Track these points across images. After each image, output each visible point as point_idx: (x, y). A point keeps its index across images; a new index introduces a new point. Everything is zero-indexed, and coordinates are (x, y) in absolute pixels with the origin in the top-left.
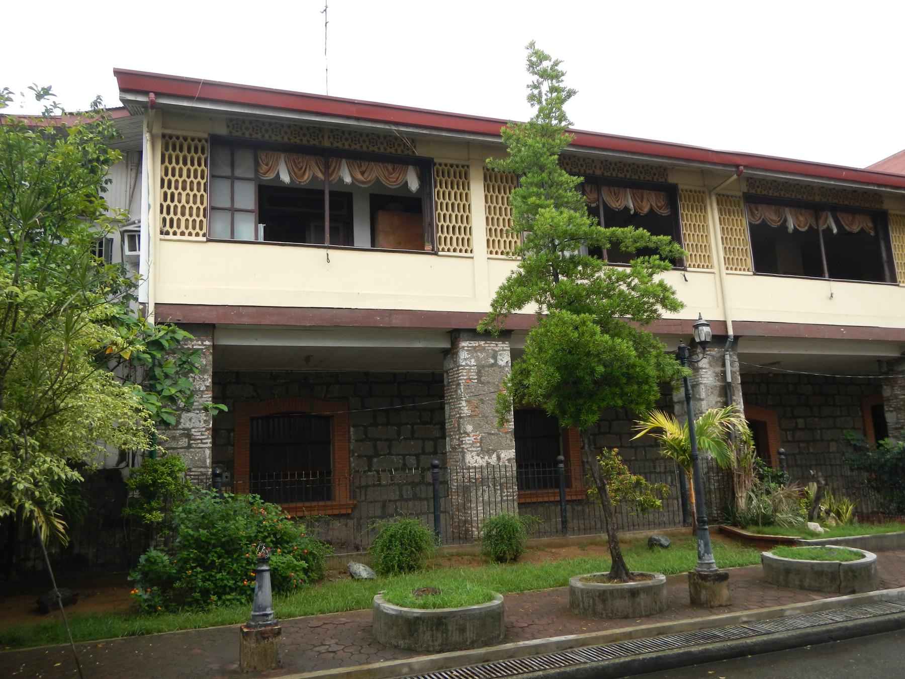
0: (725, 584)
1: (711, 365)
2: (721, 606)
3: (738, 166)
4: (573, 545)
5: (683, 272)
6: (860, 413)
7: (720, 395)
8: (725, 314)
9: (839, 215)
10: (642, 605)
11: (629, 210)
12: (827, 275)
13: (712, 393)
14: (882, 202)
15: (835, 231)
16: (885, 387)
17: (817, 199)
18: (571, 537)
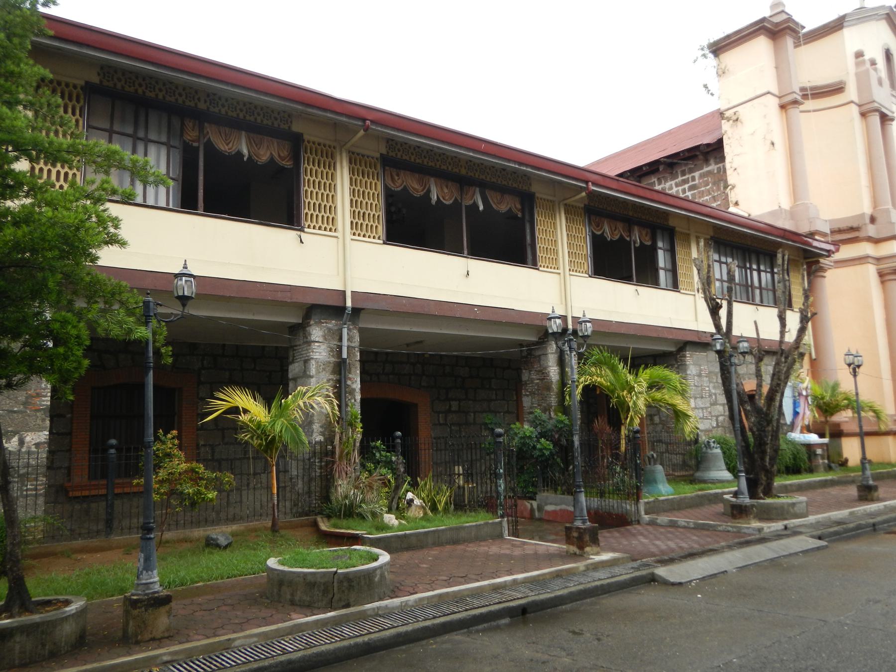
0: (163, 610)
1: (325, 339)
2: (153, 639)
3: (364, 120)
4: (118, 547)
5: (299, 233)
6: (515, 398)
7: (333, 372)
8: (345, 285)
9: (488, 193)
10: (17, 652)
11: (243, 156)
12: (466, 252)
13: (324, 369)
14: (530, 185)
15: (481, 208)
16: (524, 371)
17: (463, 172)
18: (116, 538)
